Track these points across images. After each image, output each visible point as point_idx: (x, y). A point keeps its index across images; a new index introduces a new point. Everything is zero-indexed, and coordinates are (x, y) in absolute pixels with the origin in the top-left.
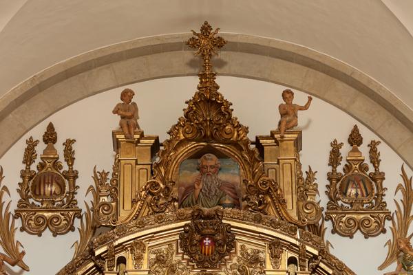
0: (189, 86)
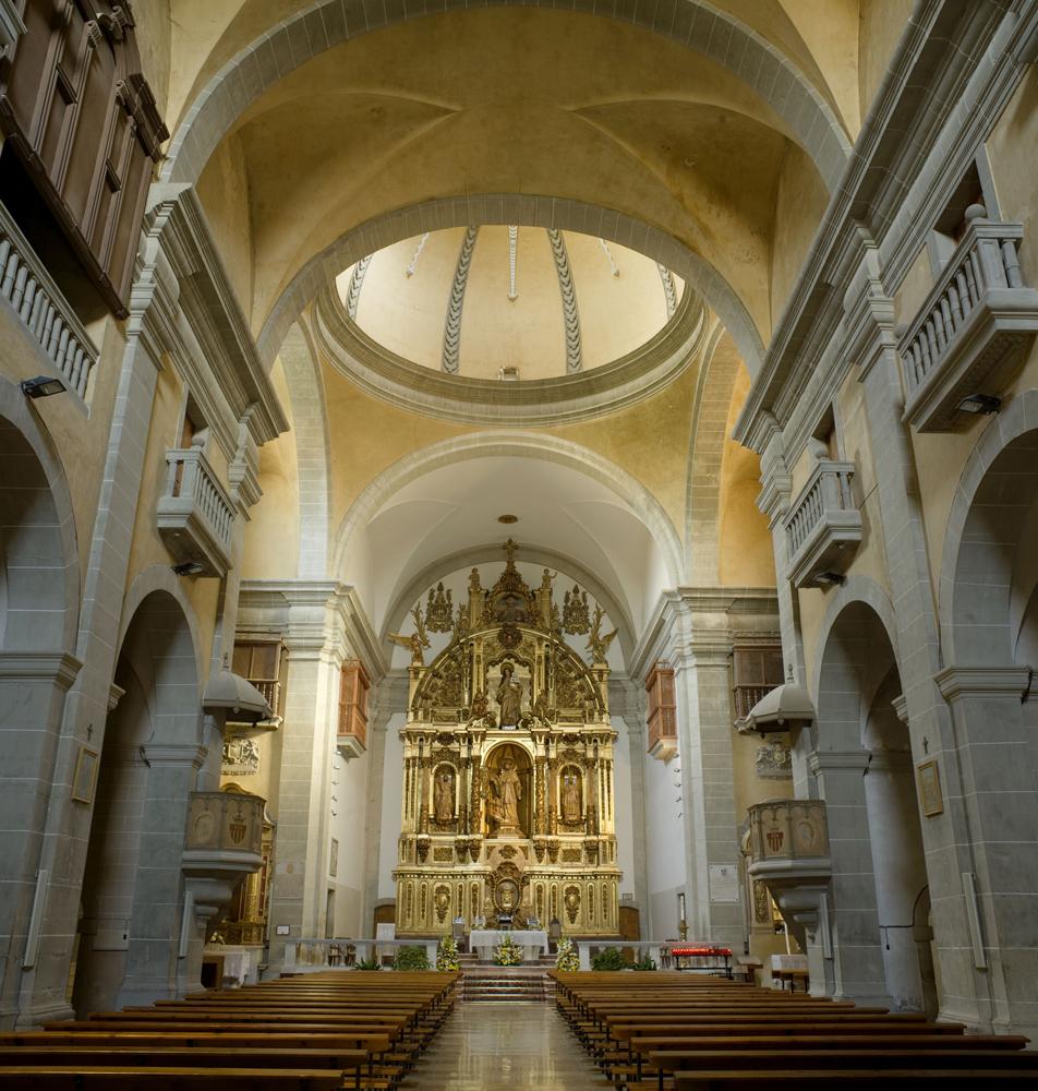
0: (502, 567)
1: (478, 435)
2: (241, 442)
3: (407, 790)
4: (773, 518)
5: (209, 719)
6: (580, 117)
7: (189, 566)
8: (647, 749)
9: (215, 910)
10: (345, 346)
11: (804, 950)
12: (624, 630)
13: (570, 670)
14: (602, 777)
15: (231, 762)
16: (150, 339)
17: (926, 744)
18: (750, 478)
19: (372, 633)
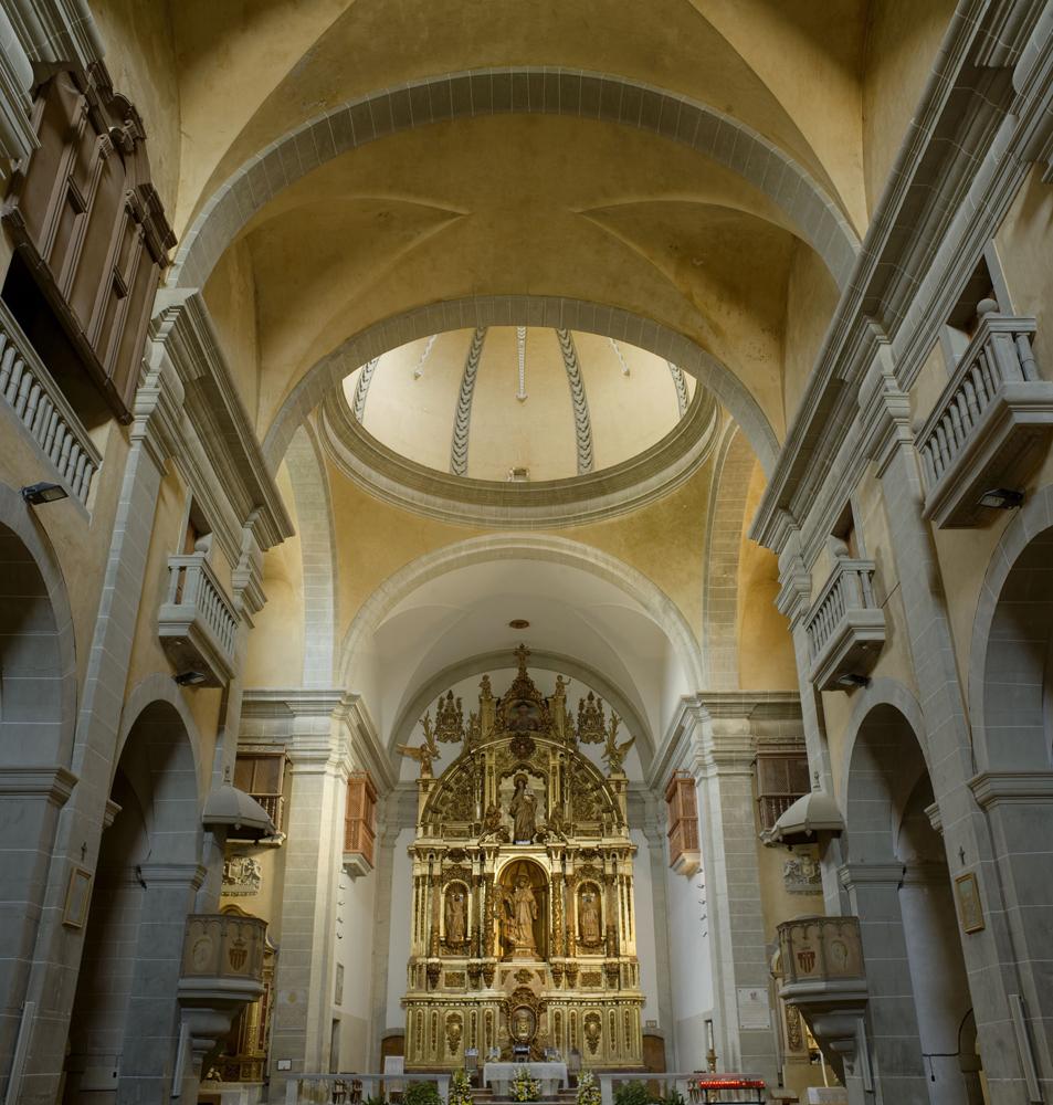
0: (514, 673)
1: (487, 538)
2: (245, 547)
3: (417, 910)
4: (793, 618)
5: (209, 836)
6: (588, 219)
7: (191, 676)
8: (669, 864)
9: (211, 1043)
10: (352, 450)
11: (843, 1082)
12: (642, 737)
13: (586, 781)
14: (622, 894)
15: (231, 882)
16: (154, 445)
17: (962, 855)
18: (769, 579)
19: (380, 744)
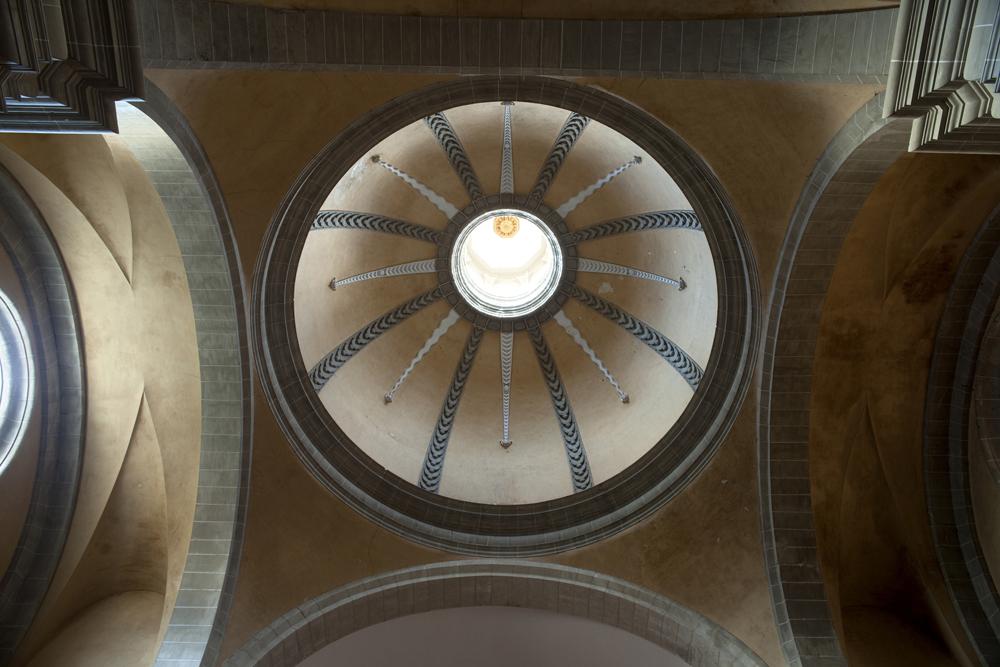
1: (458, 563)
